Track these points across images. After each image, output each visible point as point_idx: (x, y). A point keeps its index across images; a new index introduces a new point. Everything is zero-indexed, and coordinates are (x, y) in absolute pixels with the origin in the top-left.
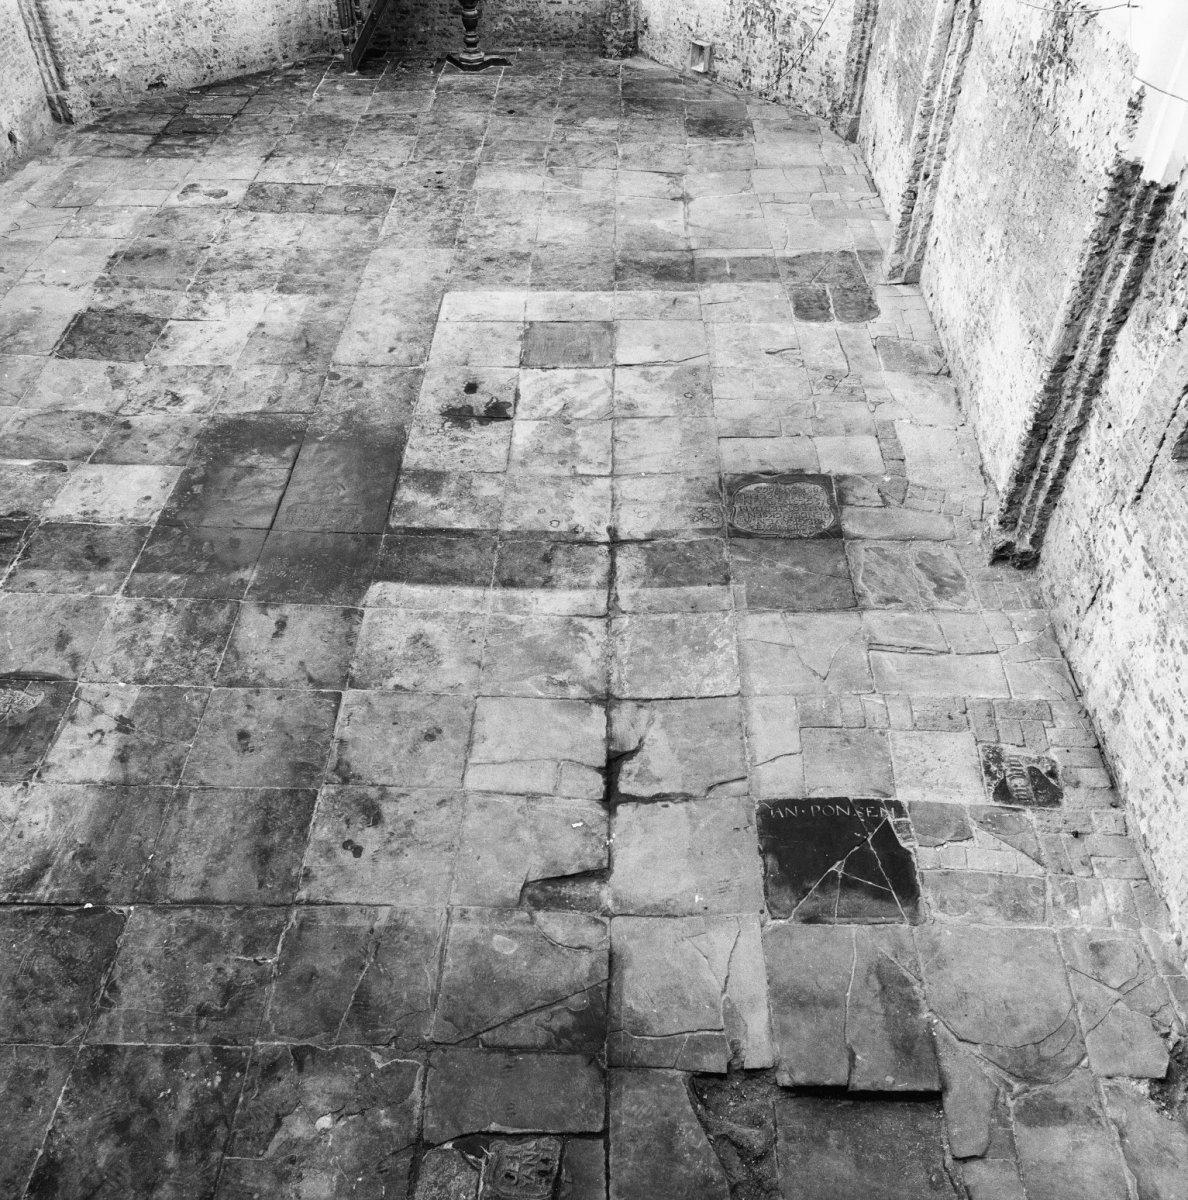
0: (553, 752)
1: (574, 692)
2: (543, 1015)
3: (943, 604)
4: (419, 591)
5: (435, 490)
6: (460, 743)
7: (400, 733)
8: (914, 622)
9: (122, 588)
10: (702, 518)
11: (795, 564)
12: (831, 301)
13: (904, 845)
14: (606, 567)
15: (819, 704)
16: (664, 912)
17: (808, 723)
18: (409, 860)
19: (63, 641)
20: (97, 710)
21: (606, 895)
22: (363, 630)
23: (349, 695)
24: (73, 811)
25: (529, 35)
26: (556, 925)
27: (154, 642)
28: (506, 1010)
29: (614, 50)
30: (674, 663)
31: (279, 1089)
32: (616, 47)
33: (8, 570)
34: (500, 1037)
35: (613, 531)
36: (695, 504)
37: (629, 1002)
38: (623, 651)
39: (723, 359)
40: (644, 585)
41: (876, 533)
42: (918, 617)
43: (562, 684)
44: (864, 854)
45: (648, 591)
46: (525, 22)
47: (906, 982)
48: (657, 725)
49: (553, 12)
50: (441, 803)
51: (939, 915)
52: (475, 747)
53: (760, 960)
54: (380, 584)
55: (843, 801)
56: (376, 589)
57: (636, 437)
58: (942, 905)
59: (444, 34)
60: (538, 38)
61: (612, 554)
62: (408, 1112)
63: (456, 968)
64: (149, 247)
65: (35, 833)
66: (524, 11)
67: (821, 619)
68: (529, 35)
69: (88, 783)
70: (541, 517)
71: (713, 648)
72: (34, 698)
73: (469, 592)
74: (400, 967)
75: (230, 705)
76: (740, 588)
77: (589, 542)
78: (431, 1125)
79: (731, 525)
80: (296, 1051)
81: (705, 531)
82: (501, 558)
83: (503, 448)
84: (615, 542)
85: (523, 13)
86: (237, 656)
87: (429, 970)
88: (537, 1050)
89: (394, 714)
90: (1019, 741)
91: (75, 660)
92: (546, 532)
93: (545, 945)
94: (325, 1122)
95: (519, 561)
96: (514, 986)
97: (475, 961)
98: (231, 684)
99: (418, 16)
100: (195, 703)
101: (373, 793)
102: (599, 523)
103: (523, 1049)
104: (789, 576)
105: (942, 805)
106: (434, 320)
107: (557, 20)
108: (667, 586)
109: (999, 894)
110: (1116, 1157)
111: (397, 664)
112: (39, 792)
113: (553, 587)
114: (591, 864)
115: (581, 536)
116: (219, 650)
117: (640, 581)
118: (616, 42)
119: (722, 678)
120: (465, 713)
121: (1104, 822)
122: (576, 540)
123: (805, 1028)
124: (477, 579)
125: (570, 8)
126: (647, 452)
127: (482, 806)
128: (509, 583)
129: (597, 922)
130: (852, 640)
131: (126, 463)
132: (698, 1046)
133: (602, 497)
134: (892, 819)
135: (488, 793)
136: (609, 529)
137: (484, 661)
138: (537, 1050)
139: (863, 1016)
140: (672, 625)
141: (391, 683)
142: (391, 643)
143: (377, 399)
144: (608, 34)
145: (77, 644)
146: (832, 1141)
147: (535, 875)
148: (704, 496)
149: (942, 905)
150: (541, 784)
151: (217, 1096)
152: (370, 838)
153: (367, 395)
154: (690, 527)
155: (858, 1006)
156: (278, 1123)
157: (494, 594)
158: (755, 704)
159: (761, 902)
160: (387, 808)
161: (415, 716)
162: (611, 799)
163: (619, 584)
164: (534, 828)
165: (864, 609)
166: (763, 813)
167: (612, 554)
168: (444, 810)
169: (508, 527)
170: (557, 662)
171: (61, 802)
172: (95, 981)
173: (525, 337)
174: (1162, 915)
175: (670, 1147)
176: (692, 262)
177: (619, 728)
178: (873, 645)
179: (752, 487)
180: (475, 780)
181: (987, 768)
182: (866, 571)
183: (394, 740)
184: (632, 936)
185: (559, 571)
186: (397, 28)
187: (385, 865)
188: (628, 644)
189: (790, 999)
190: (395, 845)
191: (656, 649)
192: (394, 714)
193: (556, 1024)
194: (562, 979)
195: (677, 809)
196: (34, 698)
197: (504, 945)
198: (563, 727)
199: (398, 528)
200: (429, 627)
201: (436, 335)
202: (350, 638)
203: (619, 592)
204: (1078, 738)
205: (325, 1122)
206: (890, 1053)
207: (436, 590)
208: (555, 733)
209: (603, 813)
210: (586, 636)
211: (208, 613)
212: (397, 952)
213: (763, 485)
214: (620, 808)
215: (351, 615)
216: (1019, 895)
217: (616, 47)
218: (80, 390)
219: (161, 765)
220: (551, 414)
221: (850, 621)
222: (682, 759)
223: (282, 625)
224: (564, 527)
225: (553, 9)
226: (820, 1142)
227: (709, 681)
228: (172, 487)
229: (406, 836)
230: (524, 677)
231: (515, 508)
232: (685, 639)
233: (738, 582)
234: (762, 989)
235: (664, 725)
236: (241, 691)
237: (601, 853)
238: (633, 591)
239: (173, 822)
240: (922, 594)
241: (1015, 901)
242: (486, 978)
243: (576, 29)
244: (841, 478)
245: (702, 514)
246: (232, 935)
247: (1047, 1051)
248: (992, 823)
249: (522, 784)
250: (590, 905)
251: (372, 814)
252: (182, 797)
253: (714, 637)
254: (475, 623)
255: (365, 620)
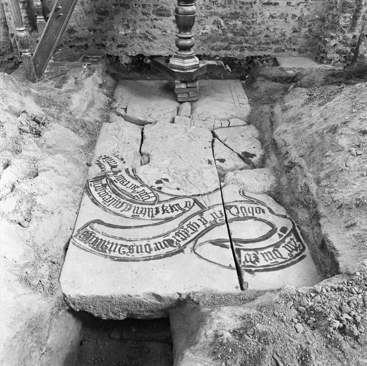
25: (238, 39)
29: (337, 55)
32: (339, 52)
46: (235, 26)
49: (267, 14)
59: (146, 37)
60: (247, 42)
66: (236, 13)
68: (238, 39)
85: (235, 15)
99: (118, 18)
107: (271, 23)
118: (341, 47)
125: (291, 11)
144: (332, 38)
186: (95, 31)
217: (339, 52)
225: (268, 11)
243: (289, 33)
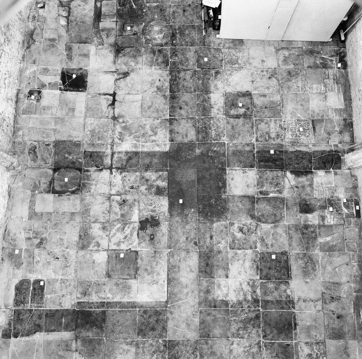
0: (125, 104)
1: (121, 120)
2: (126, 52)
3: (35, 143)
4: (157, 149)
5: (158, 188)
6: (144, 106)
7: (156, 107)
8: (44, 137)
9: (226, 145)
10: (88, 176)
11: (67, 158)
12: (30, 295)
13: (61, 82)
14: (113, 159)
15: (70, 114)
16: (106, 72)
17: (73, 110)
18: (150, 79)
19: (233, 127)
20: (218, 110)
21: (116, 76)
22: (168, 136)
23: (168, 117)
24: (214, 87)
26: (124, 69)
27: (213, 128)
28: (132, 53)
30: (99, 127)
31: (164, 41)
33: (256, 150)
34: (132, 49)
35: (111, 173)
36: (89, 182)
37: (112, 56)
38: (110, 132)
39: (72, 252)
40: (104, 152)
41: (45, 170)
42: (43, 139)
43: (124, 122)
44: (69, 80)
45: (103, 150)
47: (67, 58)
48: (104, 112)
50: (146, 91)
51: (59, 69)
52: (140, 105)
53: (90, 62)
54: (167, 151)
55: (71, 91)
56: (167, 149)
57: (103, 213)
58: (58, 70)
61: (112, 164)
62: (145, 38)
63: (140, 59)
64: (286, 335)
65: (219, 82)
67: (65, 139)
69: (213, 93)
70: (129, 178)
71: (90, 131)
72: (233, 112)
73: (145, 150)
74: (149, 59)
75: (192, 112)
76: (82, 150)
77: (118, 168)
78: (141, 36)
79: (81, 173)
80: (163, 46)
81: (88, 171)
82: (139, 162)
83: (141, 208)
84: (111, 168)
86: (194, 126)
87: (144, 59)
88: (126, 47)
89: (158, 112)
90: (32, 104)
91: (228, 123)
92: (128, 172)
93: (126, 64)
94: (157, 37)
95: (134, 161)
96: (130, 57)
97: (137, 60)
98: (192, 118)
100: (199, 113)
101: (159, 93)
102: (115, 176)
103: (128, 47)
104: (70, 154)
105: (52, 89)
106: (169, 281)
108: (99, 152)
109: (47, 72)
110: (44, 35)
111: (159, 126)
112: (223, 91)
113: (126, 152)
114: (118, 81)
115: (119, 171)
116: (198, 127)
117: (105, 154)
119: (89, 122)
120: (144, 113)
121: (23, 85)
122: (122, 169)
123: (85, 52)
124: (144, 154)
126: (101, 206)
127: (138, 91)
128: (136, 153)
129: (117, 70)
130: (59, 132)
131: (244, 196)
132: (102, 49)
133: (114, 186)
134: (62, 87)
135: (137, 94)
136: (112, 174)
137: (141, 128)
138: (126, 47)
139: (75, 53)
140: (99, 139)
141: (159, 121)
142: (161, 132)
143: (180, 231)
145: (229, 127)
146: (84, 39)
147: (128, 77)
148: (86, 185)
149: (58, 70)
150: (128, 97)
151: (173, 40)
152: (158, 84)
153: (184, 233)
154: (92, 173)
155: (76, 55)
156: (164, 37)
157: (140, 150)
158: (83, 115)
159: (88, 72)
160: (156, 89)
161: (153, 112)
162: (114, 95)
163: (110, 153)
164: (128, 87)
165: (54, 142)
166: (86, 89)
167: (112, 164)
168: (145, 89)
169: (138, 174)
170: (125, 128)
171: (217, 89)
172: (198, 56)
173: (137, 269)
174: (21, 68)
175: (107, 35)
176: (77, 327)
177: (112, 112)
178: (55, 130)
179: (74, 189)
180: (139, 97)
181: (41, 98)
182: (51, 155)
183: (157, 105)
184: (111, 67)
185: (124, 158)
187: (154, 78)
188: (109, 134)
189: (86, 56)
190: (153, 82)
191: (103, 132)
192: (158, 112)
193: (124, 51)
194: (123, 58)
195: (102, 92)
196: (233, 112)
197: (133, 64)
198: (123, 111)
199: (165, 171)
200: (153, 138)
201: (166, 270)
202: (171, 131)
203: (110, 151)
204: (20, 104)
205: (157, 37)
206: (73, 48)
207: (153, 150)
208: (125, 109)
209: (116, 92)
210: (119, 137)
211: (204, 138)
212: (150, 62)
213: (70, 190)
214: (113, 93)
215: (172, 140)
216: (44, 72)
218: (273, 235)
219: (201, 97)
220: (128, 226)
221: (59, 137)
222: (100, 103)
223: (186, 135)
224: (123, 174)
226: (86, 38)
227: (92, 122)
228: (228, 186)
229: (152, 84)
230: (132, 124)
231: (136, 181)
232: (96, 135)
233: (82, 152)
234: (91, 57)
235: (103, 111)
236: (191, 116)
237: (116, 84)
238: (107, 151)
239: (195, 86)
240: (39, 147)
241: (46, 71)
242: (135, 57)
244: (48, 192)
245: (88, 179)
246: (178, 64)
247: (49, 47)
248: (43, 86)
249: (130, 97)
250: (119, 74)
251: (158, 88)
252: (195, 91)
253: (90, 134)
254: (143, 140)
255: (168, 139)
